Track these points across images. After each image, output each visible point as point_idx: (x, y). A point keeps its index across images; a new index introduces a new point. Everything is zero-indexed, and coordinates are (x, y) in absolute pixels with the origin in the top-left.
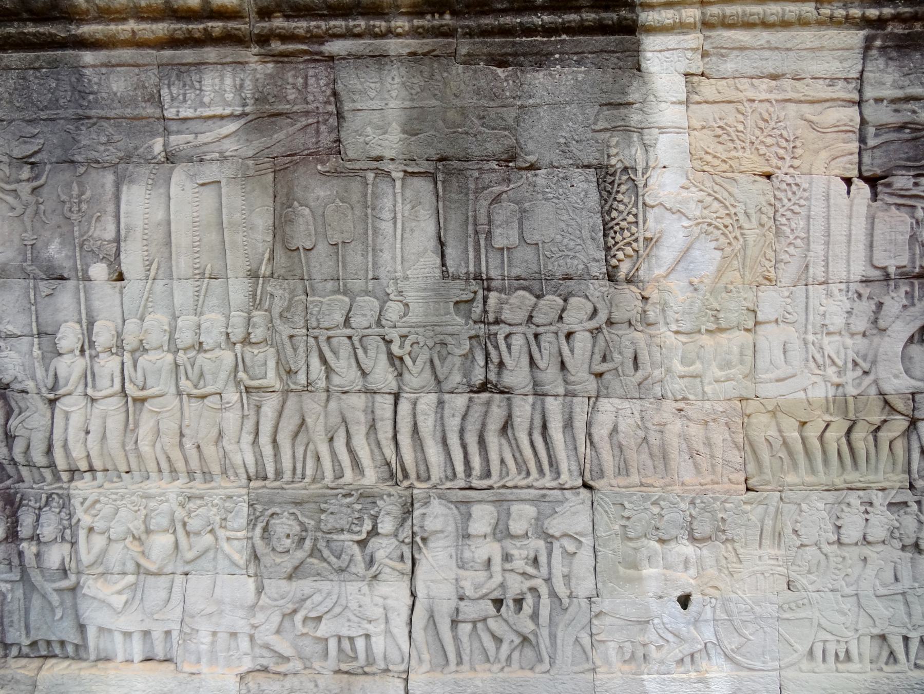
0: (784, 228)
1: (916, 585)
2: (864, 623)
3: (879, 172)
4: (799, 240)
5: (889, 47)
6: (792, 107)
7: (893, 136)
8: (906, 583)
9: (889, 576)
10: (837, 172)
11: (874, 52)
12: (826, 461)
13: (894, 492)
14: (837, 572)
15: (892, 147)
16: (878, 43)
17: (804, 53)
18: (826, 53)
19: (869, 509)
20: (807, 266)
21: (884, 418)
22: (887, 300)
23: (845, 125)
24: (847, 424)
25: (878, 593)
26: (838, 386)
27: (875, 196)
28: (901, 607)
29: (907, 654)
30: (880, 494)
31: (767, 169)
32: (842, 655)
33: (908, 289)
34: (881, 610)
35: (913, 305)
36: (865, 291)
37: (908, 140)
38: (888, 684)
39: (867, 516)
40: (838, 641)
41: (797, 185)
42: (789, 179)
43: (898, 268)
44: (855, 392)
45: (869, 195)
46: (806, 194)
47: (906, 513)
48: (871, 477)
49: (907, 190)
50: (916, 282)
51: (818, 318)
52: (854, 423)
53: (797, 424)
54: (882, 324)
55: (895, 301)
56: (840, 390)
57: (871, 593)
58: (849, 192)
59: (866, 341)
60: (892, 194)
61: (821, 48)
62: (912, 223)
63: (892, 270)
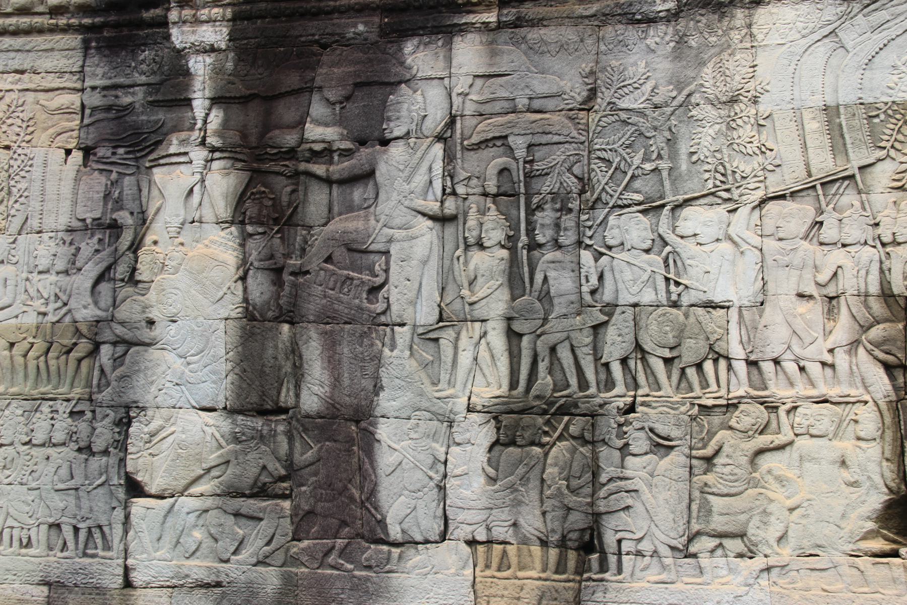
0: (13, 189)
1: (87, 482)
2: (41, 512)
3: (89, 143)
4: (23, 198)
5: (101, 47)
6: (30, 96)
7: (102, 116)
8: (77, 481)
9: (64, 472)
10: (59, 144)
11: (93, 51)
12: (26, 376)
13: (74, 402)
14: (25, 468)
15: (102, 124)
16: (93, 44)
17: (40, 53)
18: (56, 53)
19: (56, 416)
20: (27, 218)
21: (74, 341)
22: (83, 245)
23: (68, 108)
24: (46, 345)
25: (57, 487)
26: (45, 314)
27: (85, 165)
28: (72, 500)
29: (77, 543)
30: (65, 403)
31: (6, 143)
32: (25, 541)
33: (101, 237)
34: (58, 501)
35: (104, 250)
36: (68, 239)
37: (113, 119)
38: (58, 568)
39: (53, 422)
40: (23, 528)
41: (26, 155)
42: (20, 151)
43: (94, 220)
44: (55, 319)
45: (81, 163)
46: (30, 162)
47: (83, 421)
48: (60, 390)
49: (107, 158)
50: (108, 231)
51: (32, 259)
52: (52, 343)
53: (8, 344)
54: (78, 264)
55: (88, 246)
56: (46, 318)
57: (49, 487)
58: (66, 160)
59: (68, 278)
60: (98, 162)
61: (52, 50)
62: (107, 185)
63: (89, 221)
